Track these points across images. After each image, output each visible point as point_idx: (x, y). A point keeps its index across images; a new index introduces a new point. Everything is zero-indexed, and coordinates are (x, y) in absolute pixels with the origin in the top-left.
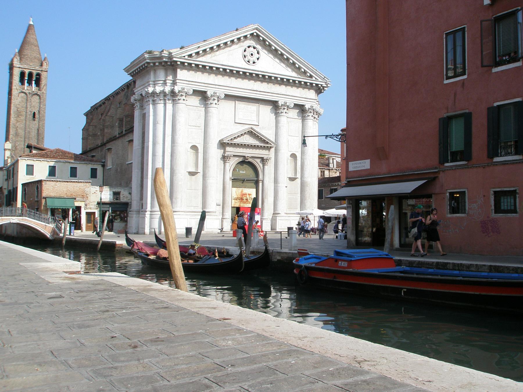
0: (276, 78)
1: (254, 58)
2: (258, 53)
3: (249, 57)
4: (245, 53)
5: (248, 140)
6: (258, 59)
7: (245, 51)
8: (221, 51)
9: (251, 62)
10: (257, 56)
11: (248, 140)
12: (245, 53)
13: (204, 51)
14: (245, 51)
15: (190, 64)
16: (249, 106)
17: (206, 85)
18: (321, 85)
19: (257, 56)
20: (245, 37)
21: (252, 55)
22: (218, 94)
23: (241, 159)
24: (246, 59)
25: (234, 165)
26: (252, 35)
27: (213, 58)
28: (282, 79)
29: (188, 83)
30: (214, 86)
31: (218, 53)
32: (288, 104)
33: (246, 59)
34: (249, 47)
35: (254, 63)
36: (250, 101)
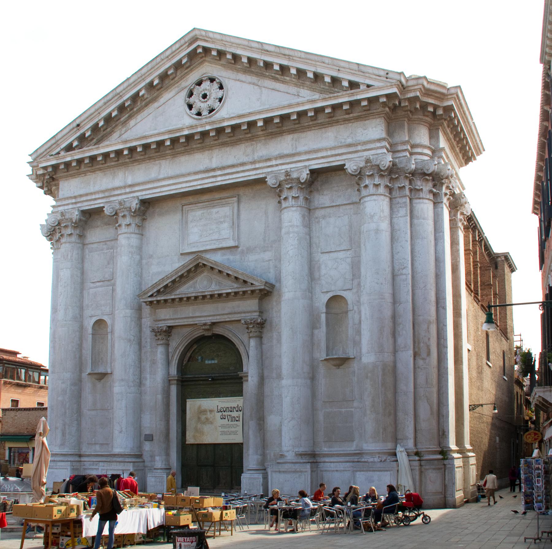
0: (252, 124)
1: (211, 102)
2: (221, 87)
3: (199, 104)
4: (192, 100)
5: (201, 285)
6: (220, 100)
7: (191, 94)
8: (139, 117)
9: (205, 113)
10: (220, 93)
11: (201, 285)
12: (192, 100)
13: (95, 128)
14: (191, 94)
15: (68, 165)
16: (214, 210)
17: (107, 194)
18: (387, 96)
19: (220, 93)
20: (178, 66)
21: (205, 96)
22: (127, 205)
23: (198, 333)
24: (194, 111)
25: (181, 348)
26: (193, 55)
27: (125, 137)
28: (268, 121)
29: (74, 201)
30: (123, 191)
31: (132, 122)
32: (295, 175)
33: (194, 111)
34: (199, 83)
35: (211, 111)
36: (217, 196)
